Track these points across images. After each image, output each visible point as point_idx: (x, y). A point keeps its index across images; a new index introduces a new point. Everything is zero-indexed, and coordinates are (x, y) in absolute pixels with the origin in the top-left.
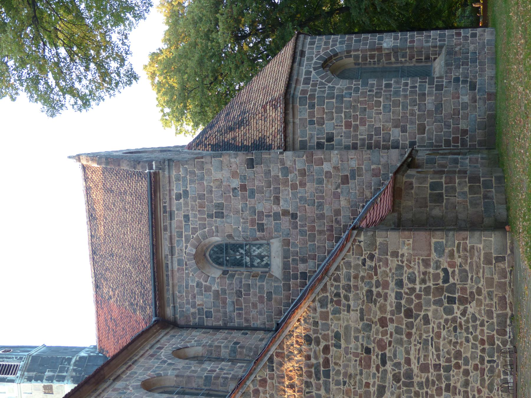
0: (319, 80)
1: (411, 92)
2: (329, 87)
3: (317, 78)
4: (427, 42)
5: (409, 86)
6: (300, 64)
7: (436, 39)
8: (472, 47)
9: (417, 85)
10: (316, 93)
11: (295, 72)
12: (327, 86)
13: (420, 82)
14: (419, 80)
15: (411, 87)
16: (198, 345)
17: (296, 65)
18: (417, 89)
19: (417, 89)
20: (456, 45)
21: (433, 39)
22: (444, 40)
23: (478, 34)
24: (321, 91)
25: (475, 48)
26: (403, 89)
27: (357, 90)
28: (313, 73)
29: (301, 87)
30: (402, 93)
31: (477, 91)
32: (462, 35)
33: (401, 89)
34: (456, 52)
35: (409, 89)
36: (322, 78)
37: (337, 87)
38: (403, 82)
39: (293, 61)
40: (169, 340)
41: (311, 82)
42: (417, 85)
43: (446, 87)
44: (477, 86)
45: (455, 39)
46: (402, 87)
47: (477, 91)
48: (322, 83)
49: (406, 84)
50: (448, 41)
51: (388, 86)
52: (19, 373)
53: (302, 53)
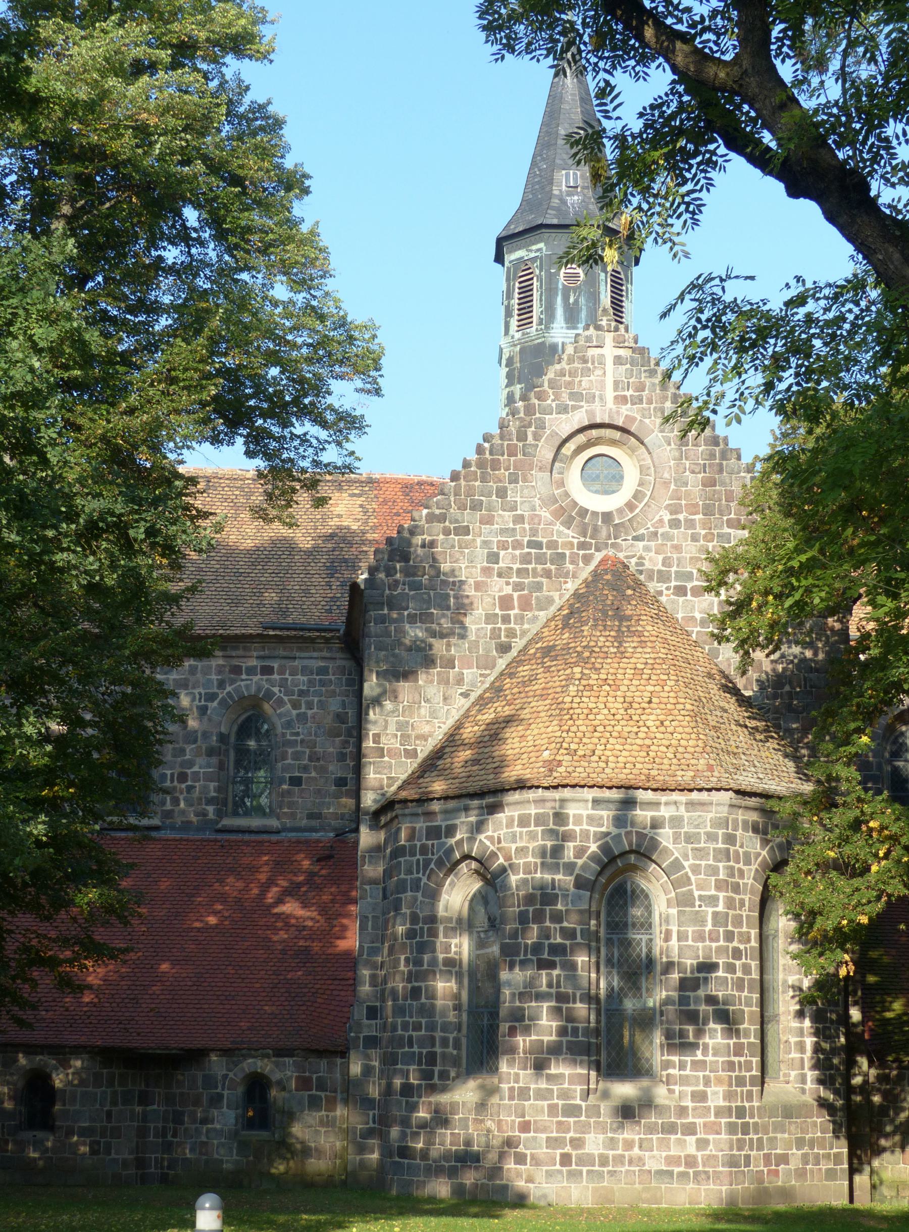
0: (435, 857)
1: (402, 1038)
2: (420, 879)
3: (438, 851)
5: (414, 1034)
7: (517, 1081)
9: (416, 1049)
10: (408, 858)
12: (420, 875)
13: (420, 1054)
14: (424, 1051)
15: (410, 1038)
18: (407, 1049)
19: (407, 1049)
21: (517, 1075)
22: (511, 1098)
23: (523, 1167)
24: (412, 866)
26: (408, 1022)
30: (399, 1020)
31: (397, 1159)
32: (523, 1135)
33: (407, 1019)
34: (482, 1121)
35: (407, 1034)
37: (419, 895)
38: (423, 1021)
40: (305, 670)
41: (430, 842)
42: (416, 1049)
43: (407, 1102)
44: (406, 1161)
45: (514, 1121)
46: (411, 1020)
47: (397, 1159)
50: (511, 1106)
52: (518, 335)
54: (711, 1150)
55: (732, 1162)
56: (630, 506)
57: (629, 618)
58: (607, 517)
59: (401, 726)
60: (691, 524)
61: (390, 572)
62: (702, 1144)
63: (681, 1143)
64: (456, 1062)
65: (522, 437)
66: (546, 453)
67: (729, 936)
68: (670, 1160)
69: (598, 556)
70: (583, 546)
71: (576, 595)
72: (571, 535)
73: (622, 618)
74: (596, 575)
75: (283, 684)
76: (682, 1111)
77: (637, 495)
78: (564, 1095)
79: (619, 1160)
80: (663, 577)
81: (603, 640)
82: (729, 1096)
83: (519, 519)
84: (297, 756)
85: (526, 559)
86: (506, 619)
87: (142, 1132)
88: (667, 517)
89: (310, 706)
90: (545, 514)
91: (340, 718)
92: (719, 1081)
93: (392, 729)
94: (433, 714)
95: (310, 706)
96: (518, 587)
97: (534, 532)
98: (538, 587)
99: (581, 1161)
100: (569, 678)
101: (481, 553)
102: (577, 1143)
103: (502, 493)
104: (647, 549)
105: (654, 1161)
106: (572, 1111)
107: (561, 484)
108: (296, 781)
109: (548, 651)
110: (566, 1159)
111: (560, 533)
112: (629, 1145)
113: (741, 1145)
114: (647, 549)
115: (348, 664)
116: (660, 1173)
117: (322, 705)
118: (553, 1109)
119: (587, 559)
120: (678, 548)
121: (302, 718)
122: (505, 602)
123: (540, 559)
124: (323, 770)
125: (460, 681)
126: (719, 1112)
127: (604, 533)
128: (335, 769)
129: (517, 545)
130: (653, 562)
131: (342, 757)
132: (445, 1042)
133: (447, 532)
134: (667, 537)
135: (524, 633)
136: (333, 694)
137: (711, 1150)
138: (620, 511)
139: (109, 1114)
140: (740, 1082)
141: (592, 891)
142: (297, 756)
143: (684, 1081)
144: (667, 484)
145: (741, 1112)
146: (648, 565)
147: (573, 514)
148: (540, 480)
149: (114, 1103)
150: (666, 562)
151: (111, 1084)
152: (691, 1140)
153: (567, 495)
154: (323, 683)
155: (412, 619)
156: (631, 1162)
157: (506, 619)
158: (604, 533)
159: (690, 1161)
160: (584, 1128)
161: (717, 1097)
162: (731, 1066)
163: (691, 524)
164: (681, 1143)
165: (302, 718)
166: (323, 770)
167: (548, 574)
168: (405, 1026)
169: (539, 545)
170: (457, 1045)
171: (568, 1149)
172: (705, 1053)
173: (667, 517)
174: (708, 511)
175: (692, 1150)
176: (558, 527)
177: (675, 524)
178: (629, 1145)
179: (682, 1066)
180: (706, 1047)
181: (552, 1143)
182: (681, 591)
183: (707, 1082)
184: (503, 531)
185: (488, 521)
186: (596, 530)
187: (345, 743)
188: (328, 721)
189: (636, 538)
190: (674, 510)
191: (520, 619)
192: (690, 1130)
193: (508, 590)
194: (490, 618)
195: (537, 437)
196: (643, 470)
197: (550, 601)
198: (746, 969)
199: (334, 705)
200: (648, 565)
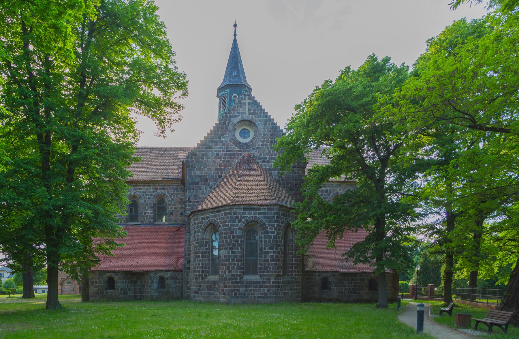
4: (222, 272)
6: (211, 212)
8: (217, 293)
11: (207, 212)
16: (169, 201)
17: (211, 210)
20: (219, 286)
22: (222, 280)
25: (217, 294)
27: (197, 243)
28: (207, 220)
29: (200, 217)
36: (204, 225)
39: (212, 209)
48: (201, 226)
49: (199, 264)
51: (199, 257)
53: (219, 211)
54: (271, 291)
55: (276, 294)
56: (252, 141)
57: (252, 167)
58: (246, 144)
59: (195, 195)
60: (267, 145)
61: (192, 158)
62: (269, 290)
63: (264, 290)
64: (208, 272)
65: (225, 124)
66: (231, 127)
67: (277, 241)
68: (261, 294)
69: (244, 153)
70: (240, 151)
71: (238, 162)
72: (237, 148)
73: (250, 167)
74: (243, 157)
75: (168, 192)
76: (264, 282)
77: (254, 138)
78: (235, 279)
79: (248, 294)
80: (260, 158)
81: (245, 171)
82: (275, 279)
83: (224, 145)
84: (171, 208)
85: (225, 154)
86: (220, 169)
87: (136, 289)
88: (261, 143)
89: (174, 197)
90: (230, 143)
91: (181, 199)
92: (273, 275)
93: (192, 196)
94: (203, 192)
95: (174, 197)
96: (223, 161)
97: (227, 148)
98: (228, 161)
99: (239, 294)
100: (237, 181)
101: (214, 153)
102: (238, 290)
103: (220, 138)
104: (256, 151)
105: (257, 294)
106: (238, 283)
107: (234, 136)
108: (171, 214)
109: (231, 175)
110: (235, 294)
111: (234, 148)
112: (251, 290)
113: (278, 290)
114: (256, 151)
115: (183, 187)
116: (258, 297)
117: (177, 196)
118: (232, 283)
119: (241, 154)
120: (263, 151)
121: (172, 199)
122: (220, 165)
123: (229, 154)
124: (177, 211)
125: (209, 184)
126: (273, 283)
127: (245, 148)
128: (180, 211)
129: (224, 151)
130: (258, 154)
131: (182, 208)
132: (206, 268)
133: (206, 148)
134: (261, 148)
135: (225, 173)
136: (179, 194)
137: (271, 291)
138: (249, 142)
139: (127, 286)
140: (278, 275)
141: (243, 230)
142: (171, 208)
143: (265, 275)
144: (261, 135)
145: (278, 283)
146: (256, 155)
147: (237, 143)
148: (229, 135)
149: (129, 283)
150: (261, 155)
151: (128, 279)
152: (266, 289)
153: (236, 138)
154: (177, 191)
155: (197, 170)
156: (251, 294)
157: (220, 169)
158: (245, 148)
159: (266, 294)
160: (240, 287)
161: (273, 279)
162: (276, 272)
163: (267, 145)
164: (264, 290)
165: (172, 199)
166: (177, 211)
167: (231, 158)
168: (196, 264)
169: (229, 151)
170: (209, 268)
171: (236, 292)
172: (270, 269)
173: (261, 143)
174: (271, 142)
175: (266, 291)
176: (234, 146)
177: (263, 145)
178: (251, 290)
179: (264, 272)
180: (270, 267)
181: (232, 290)
182: (264, 162)
183: (270, 275)
184: (220, 148)
185: (216, 145)
186: (243, 147)
187: (182, 205)
188: (178, 200)
189: (254, 149)
190: (263, 142)
191: (224, 169)
192: (266, 287)
193: (221, 162)
194: (217, 169)
195: (229, 124)
196: (255, 132)
197: (232, 165)
198: (281, 249)
199: (180, 196)
200: (256, 155)
